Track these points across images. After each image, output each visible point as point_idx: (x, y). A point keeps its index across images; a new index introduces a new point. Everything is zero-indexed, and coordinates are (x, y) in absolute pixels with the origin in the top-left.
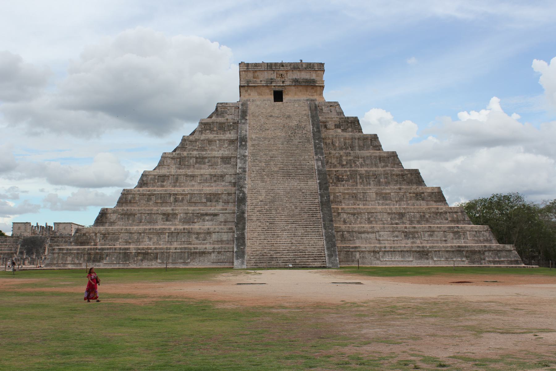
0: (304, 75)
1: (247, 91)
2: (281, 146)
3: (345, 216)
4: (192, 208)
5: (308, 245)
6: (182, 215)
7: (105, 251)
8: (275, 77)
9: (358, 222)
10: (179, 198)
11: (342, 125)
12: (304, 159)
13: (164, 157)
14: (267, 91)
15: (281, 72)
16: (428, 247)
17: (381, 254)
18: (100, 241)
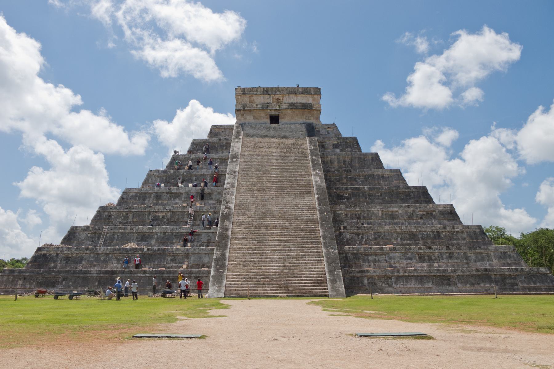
0: (301, 99)
1: (242, 115)
2: (275, 163)
3: (348, 236)
4: (172, 227)
5: (305, 268)
6: (159, 235)
7: (62, 274)
8: (271, 102)
9: (363, 243)
10: (159, 216)
11: (340, 145)
12: (301, 175)
13: (151, 175)
14: (262, 114)
15: (277, 96)
16: (449, 271)
17: (393, 279)
18: (60, 263)
